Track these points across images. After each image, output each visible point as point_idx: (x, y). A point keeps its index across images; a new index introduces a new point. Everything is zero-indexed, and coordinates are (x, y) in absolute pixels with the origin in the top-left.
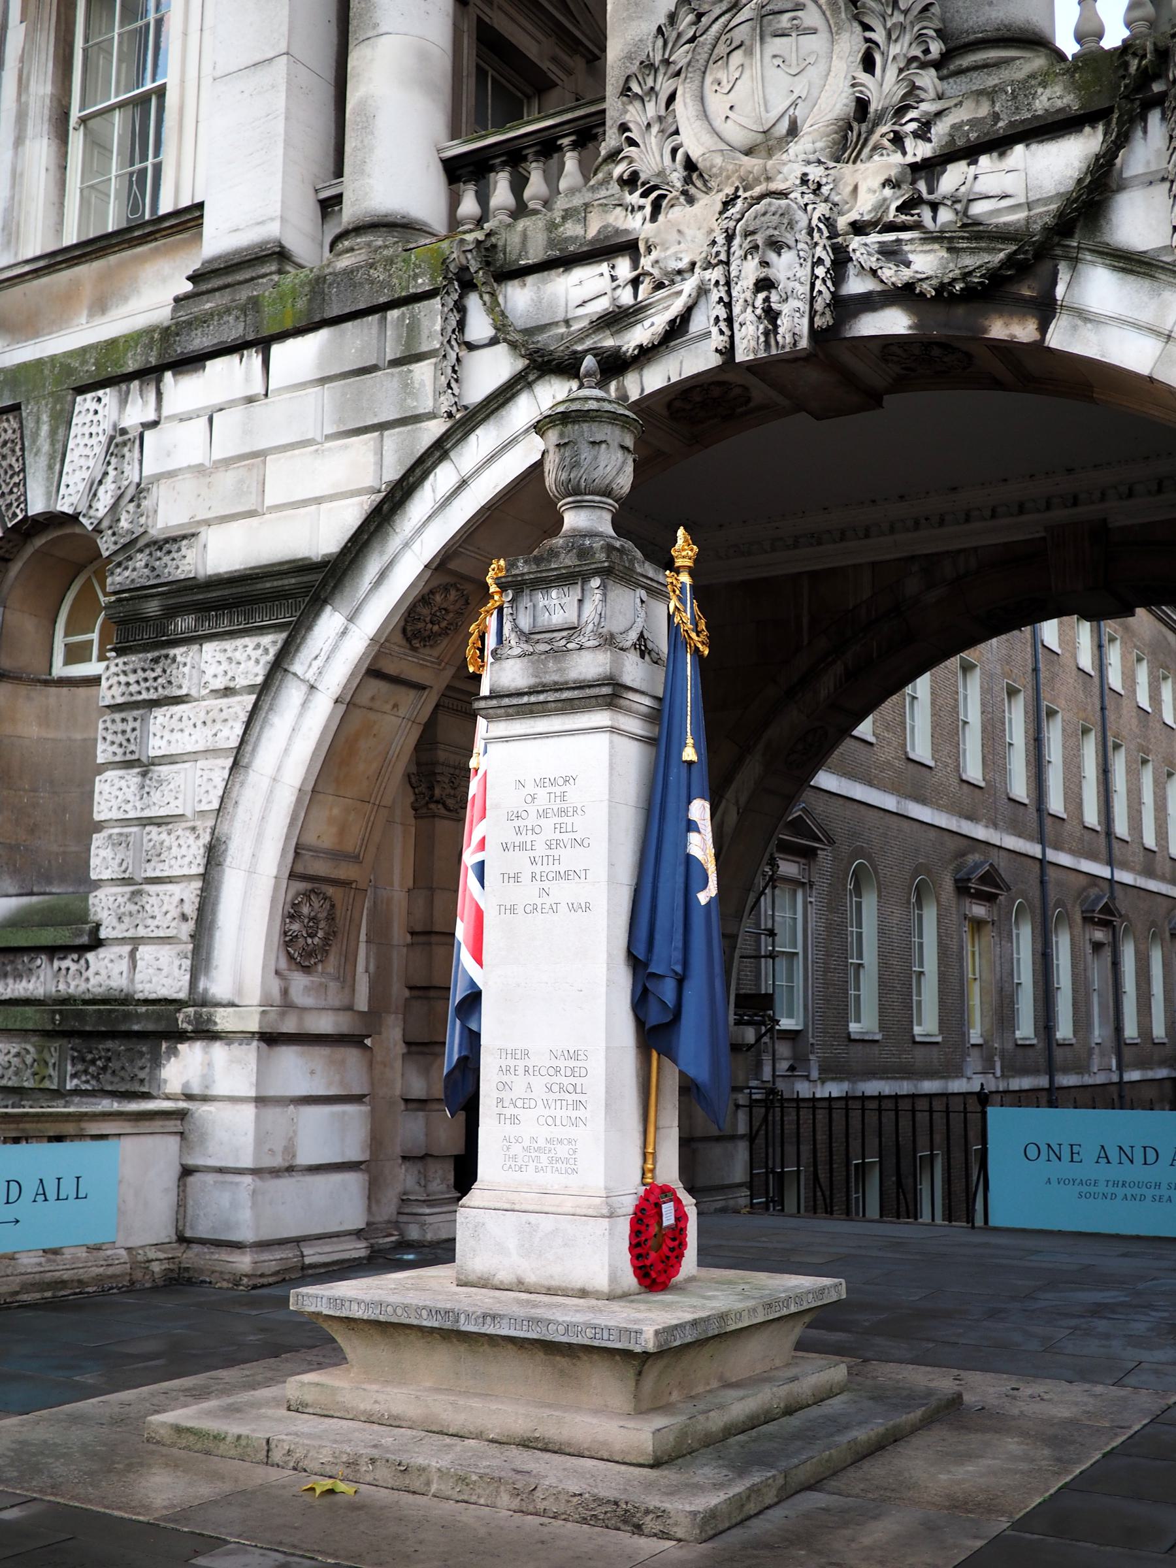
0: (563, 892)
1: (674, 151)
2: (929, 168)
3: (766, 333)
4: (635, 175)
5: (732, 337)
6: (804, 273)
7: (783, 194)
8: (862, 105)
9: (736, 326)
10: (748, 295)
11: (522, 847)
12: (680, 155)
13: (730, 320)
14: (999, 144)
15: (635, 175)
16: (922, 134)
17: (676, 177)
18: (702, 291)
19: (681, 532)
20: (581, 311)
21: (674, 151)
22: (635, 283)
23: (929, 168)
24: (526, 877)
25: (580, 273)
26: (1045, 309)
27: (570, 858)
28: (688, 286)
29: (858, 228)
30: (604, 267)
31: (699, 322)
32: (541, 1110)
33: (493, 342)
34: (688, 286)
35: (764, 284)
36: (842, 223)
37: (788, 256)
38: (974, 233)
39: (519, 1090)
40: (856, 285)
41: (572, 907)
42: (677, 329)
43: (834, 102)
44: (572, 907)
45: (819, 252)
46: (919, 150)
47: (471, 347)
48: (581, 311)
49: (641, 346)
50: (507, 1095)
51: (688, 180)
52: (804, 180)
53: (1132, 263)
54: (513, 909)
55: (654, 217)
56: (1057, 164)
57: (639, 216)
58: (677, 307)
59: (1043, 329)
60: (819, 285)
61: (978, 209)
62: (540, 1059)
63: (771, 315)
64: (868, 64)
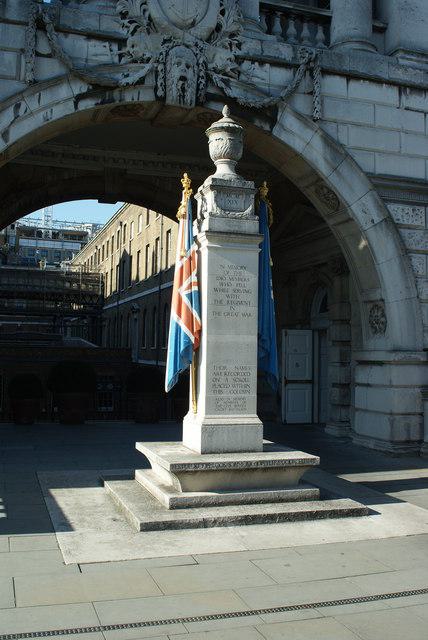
0: (242, 309)
1: (144, 11)
2: (239, 60)
3: (180, 96)
4: (127, 13)
5: (165, 93)
6: (195, 79)
7: (187, 46)
8: (218, 28)
9: (168, 89)
10: (176, 81)
11: (223, 290)
12: (147, 14)
13: (165, 86)
14: (262, 63)
15: (127, 13)
16: (239, 46)
17: (145, 22)
18: (150, 71)
19: (265, 183)
20: (94, 58)
21: (144, 11)
22: (121, 56)
23: (239, 60)
24: (225, 302)
25: (93, 42)
26: (273, 121)
27: (243, 297)
28: (148, 67)
29: (215, 70)
30: (107, 44)
31: (150, 81)
32: (231, 388)
33: (49, 56)
34: (148, 67)
35: (183, 78)
36: (210, 66)
37: (190, 71)
38: (250, 87)
39: (222, 381)
40: (211, 90)
41: (244, 315)
42: (141, 81)
43: (210, 22)
44: (244, 315)
45: (202, 74)
46: (239, 53)
47: (38, 54)
48: (94, 58)
49: (128, 84)
50: (217, 383)
51: (149, 25)
52: (196, 45)
53: (299, 116)
54: (219, 314)
55: (133, 34)
56: (279, 76)
57: (126, 30)
58: (142, 73)
59: (272, 127)
60: (201, 86)
61: (255, 80)
62: (231, 368)
63: (183, 90)
64: (222, 13)
